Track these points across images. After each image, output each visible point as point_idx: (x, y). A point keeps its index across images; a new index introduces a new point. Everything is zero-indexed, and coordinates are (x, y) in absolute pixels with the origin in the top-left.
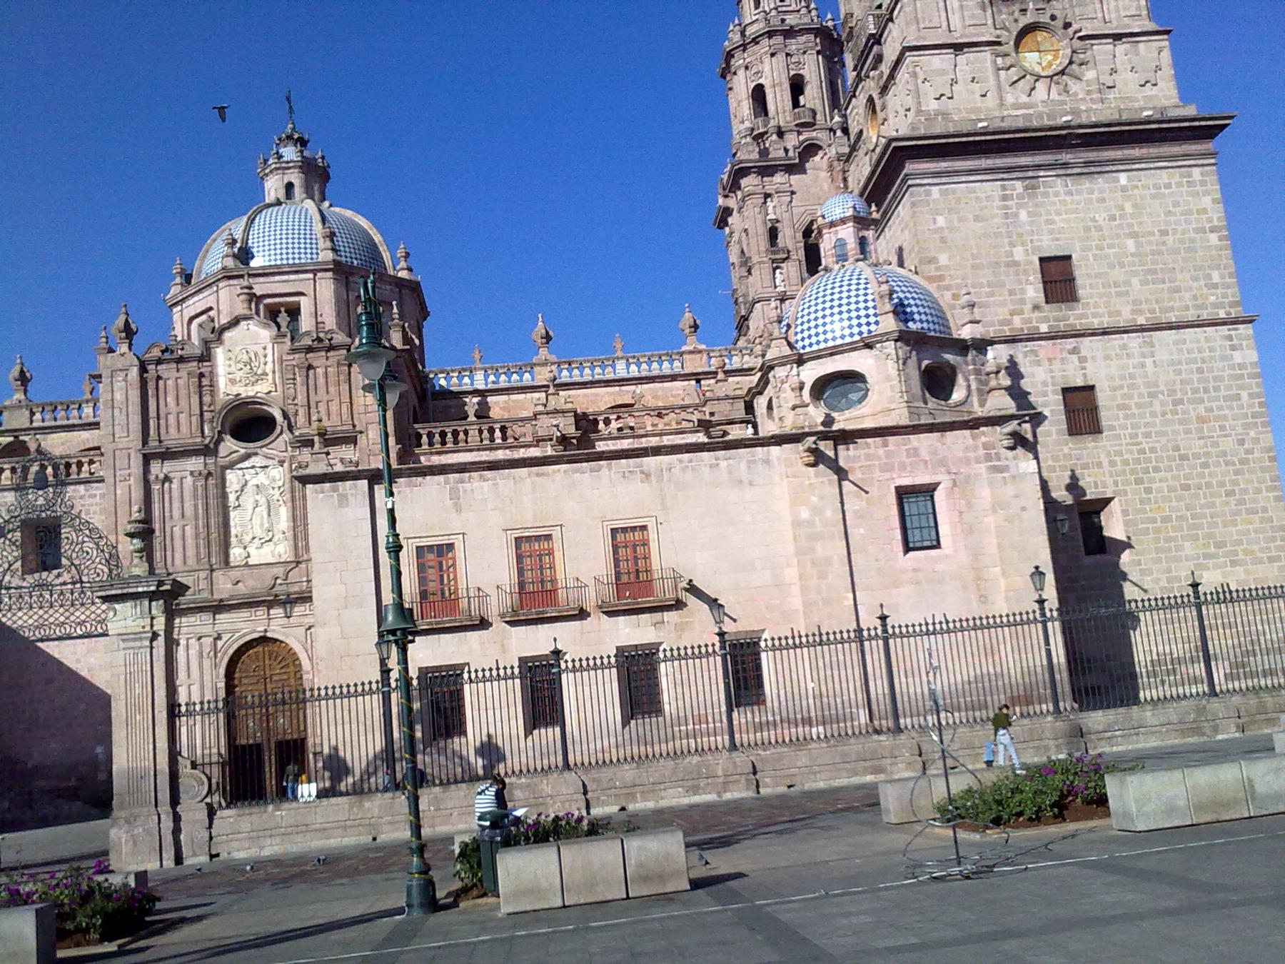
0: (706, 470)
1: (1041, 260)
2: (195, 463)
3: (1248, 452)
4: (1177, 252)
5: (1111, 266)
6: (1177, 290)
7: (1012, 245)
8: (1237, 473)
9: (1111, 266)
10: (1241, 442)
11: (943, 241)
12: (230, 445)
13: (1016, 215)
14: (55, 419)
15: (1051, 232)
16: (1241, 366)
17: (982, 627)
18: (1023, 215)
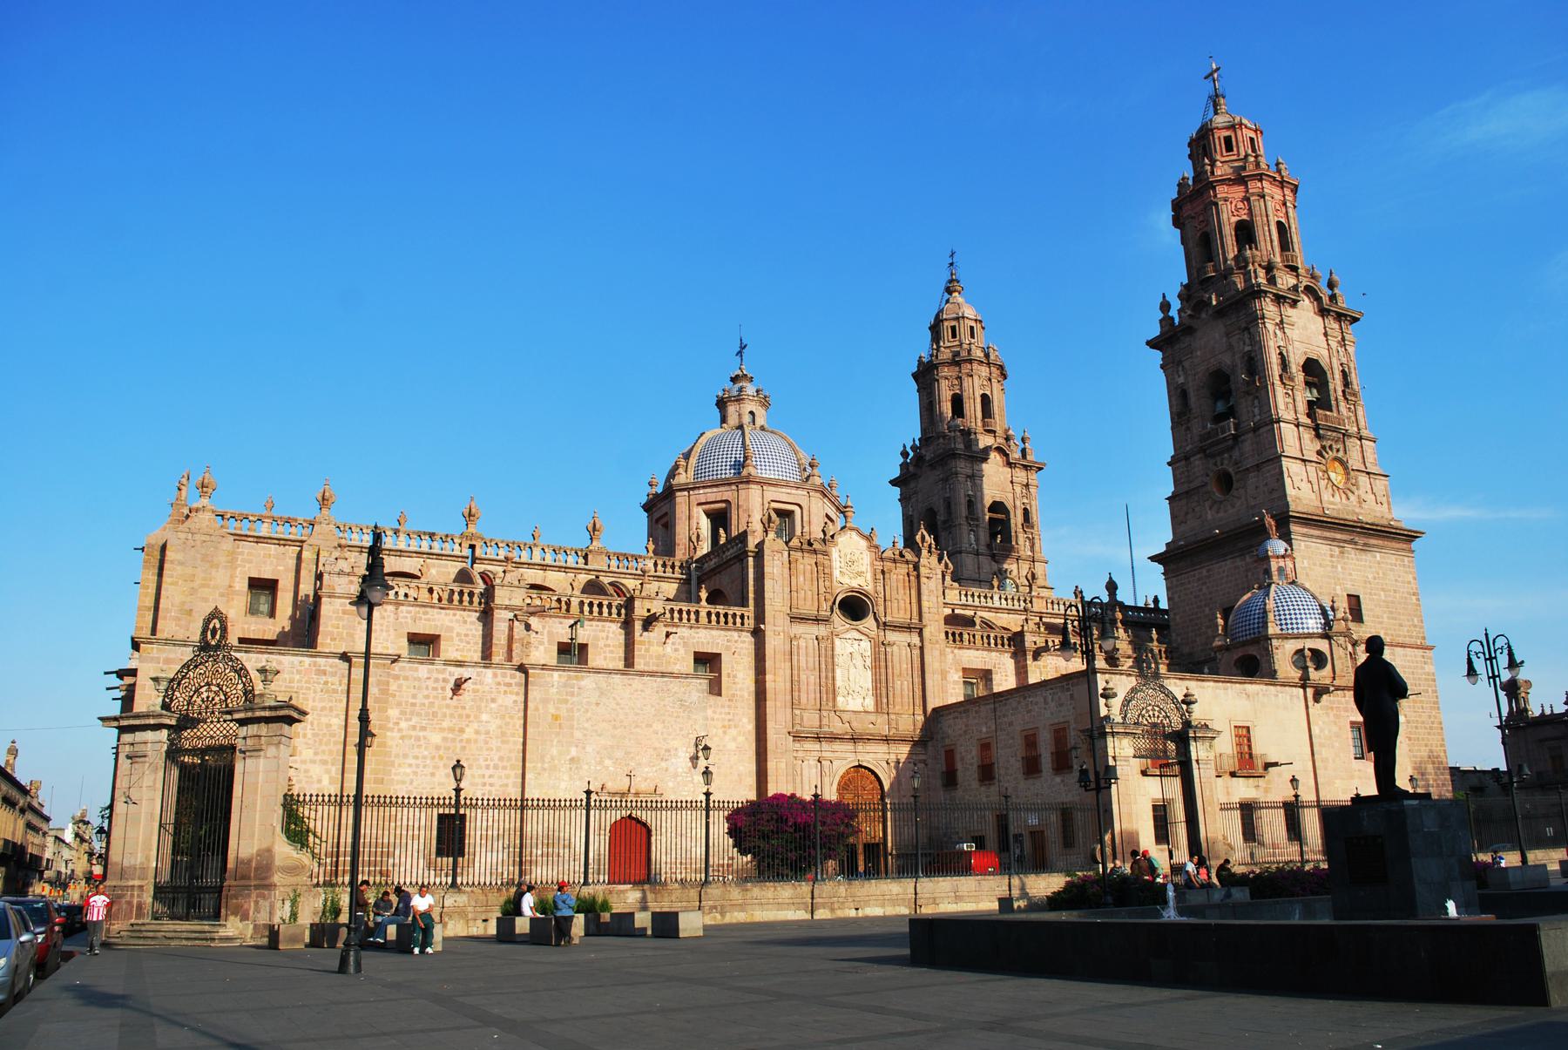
0: (1273, 698)
1: (1348, 595)
2: (822, 630)
3: (1433, 723)
4: (1400, 603)
5: (1376, 606)
6: (1401, 625)
7: (1336, 584)
8: (1429, 734)
9: (1376, 606)
10: (1430, 717)
11: (1307, 575)
12: (839, 620)
13: (1336, 567)
14: (664, 572)
15: (1351, 580)
16: (1428, 674)
17: (1228, 809)
18: (1340, 569)
